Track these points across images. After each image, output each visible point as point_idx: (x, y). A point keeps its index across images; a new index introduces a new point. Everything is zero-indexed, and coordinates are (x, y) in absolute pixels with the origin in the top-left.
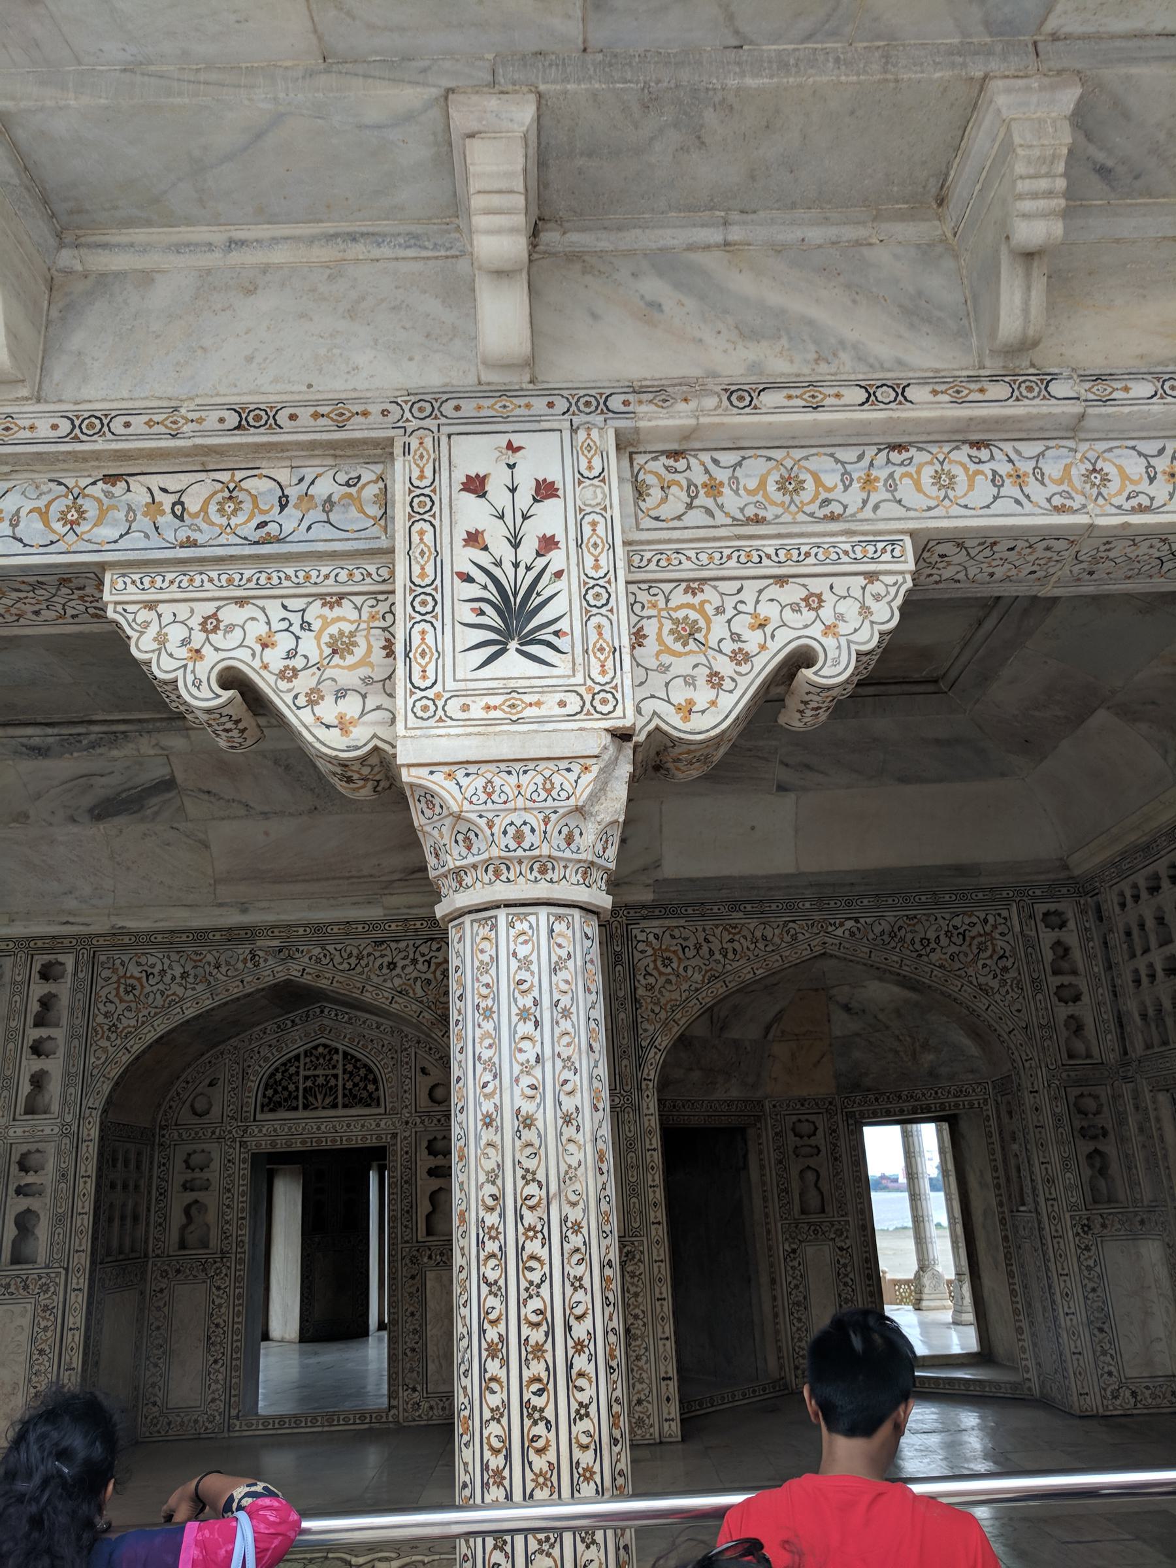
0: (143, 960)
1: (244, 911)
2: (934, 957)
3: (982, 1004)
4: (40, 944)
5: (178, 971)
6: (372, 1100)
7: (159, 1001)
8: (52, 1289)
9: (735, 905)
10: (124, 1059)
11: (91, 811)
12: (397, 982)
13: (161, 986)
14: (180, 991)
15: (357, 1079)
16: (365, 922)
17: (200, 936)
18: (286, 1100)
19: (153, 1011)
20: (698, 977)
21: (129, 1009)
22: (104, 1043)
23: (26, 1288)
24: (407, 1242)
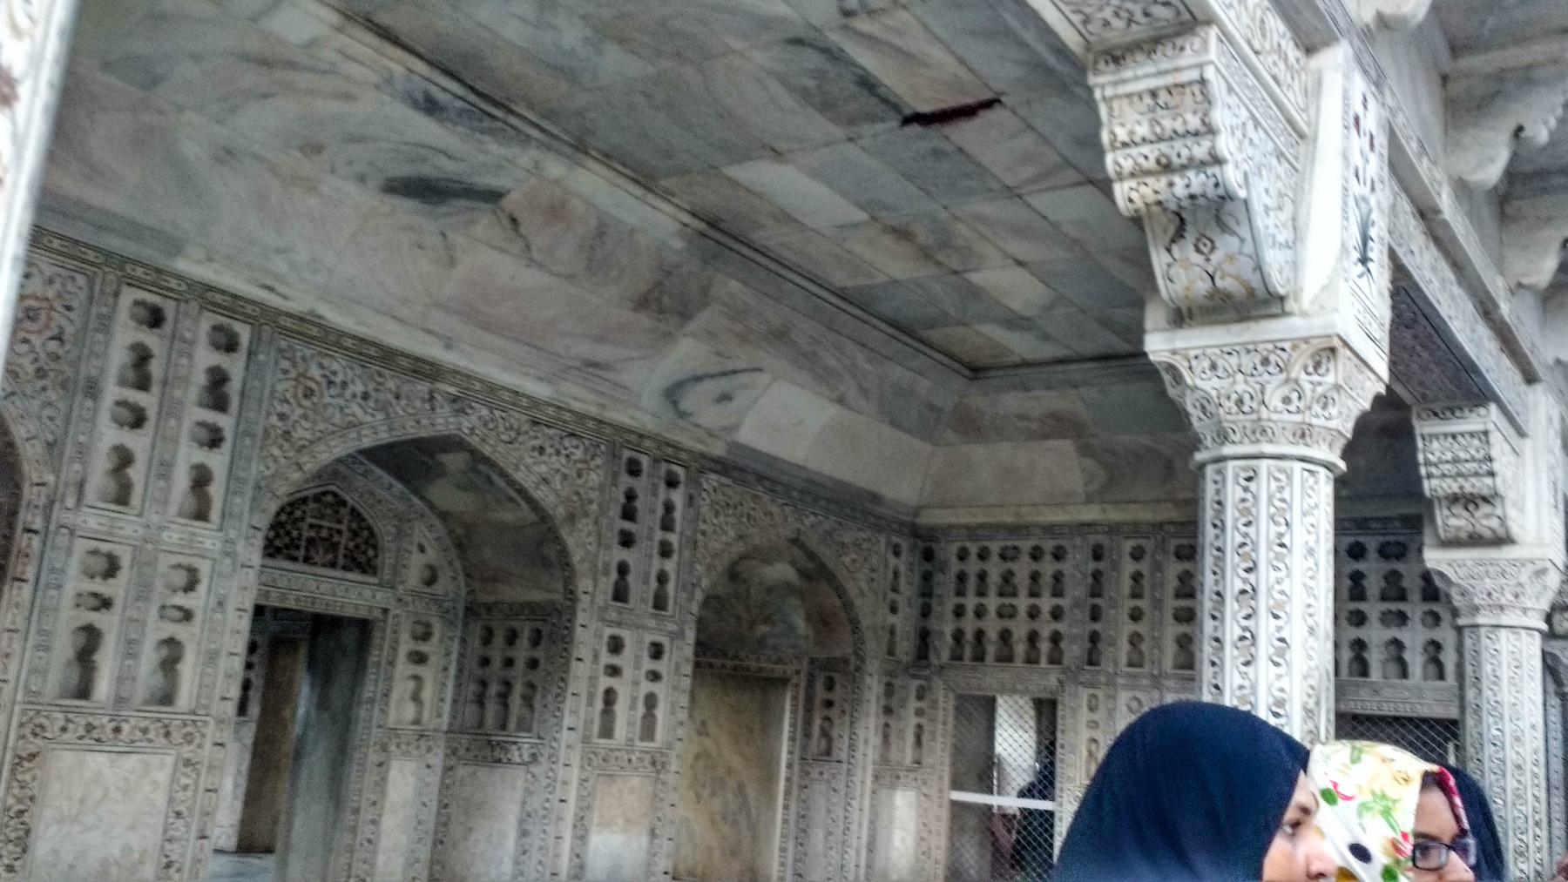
0: (326, 362)
1: (448, 347)
2: (847, 560)
3: (858, 602)
4: (218, 298)
5: (359, 388)
6: (368, 568)
7: (337, 419)
8: (197, 741)
9: (761, 478)
10: (297, 476)
11: (388, 180)
12: (544, 469)
13: (341, 401)
14: (358, 412)
15: (359, 540)
16: (529, 397)
17: (388, 356)
18: (287, 547)
19: (331, 428)
20: (732, 533)
21: (305, 417)
22: (276, 452)
23: (167, 734)
24: (380, 727)
